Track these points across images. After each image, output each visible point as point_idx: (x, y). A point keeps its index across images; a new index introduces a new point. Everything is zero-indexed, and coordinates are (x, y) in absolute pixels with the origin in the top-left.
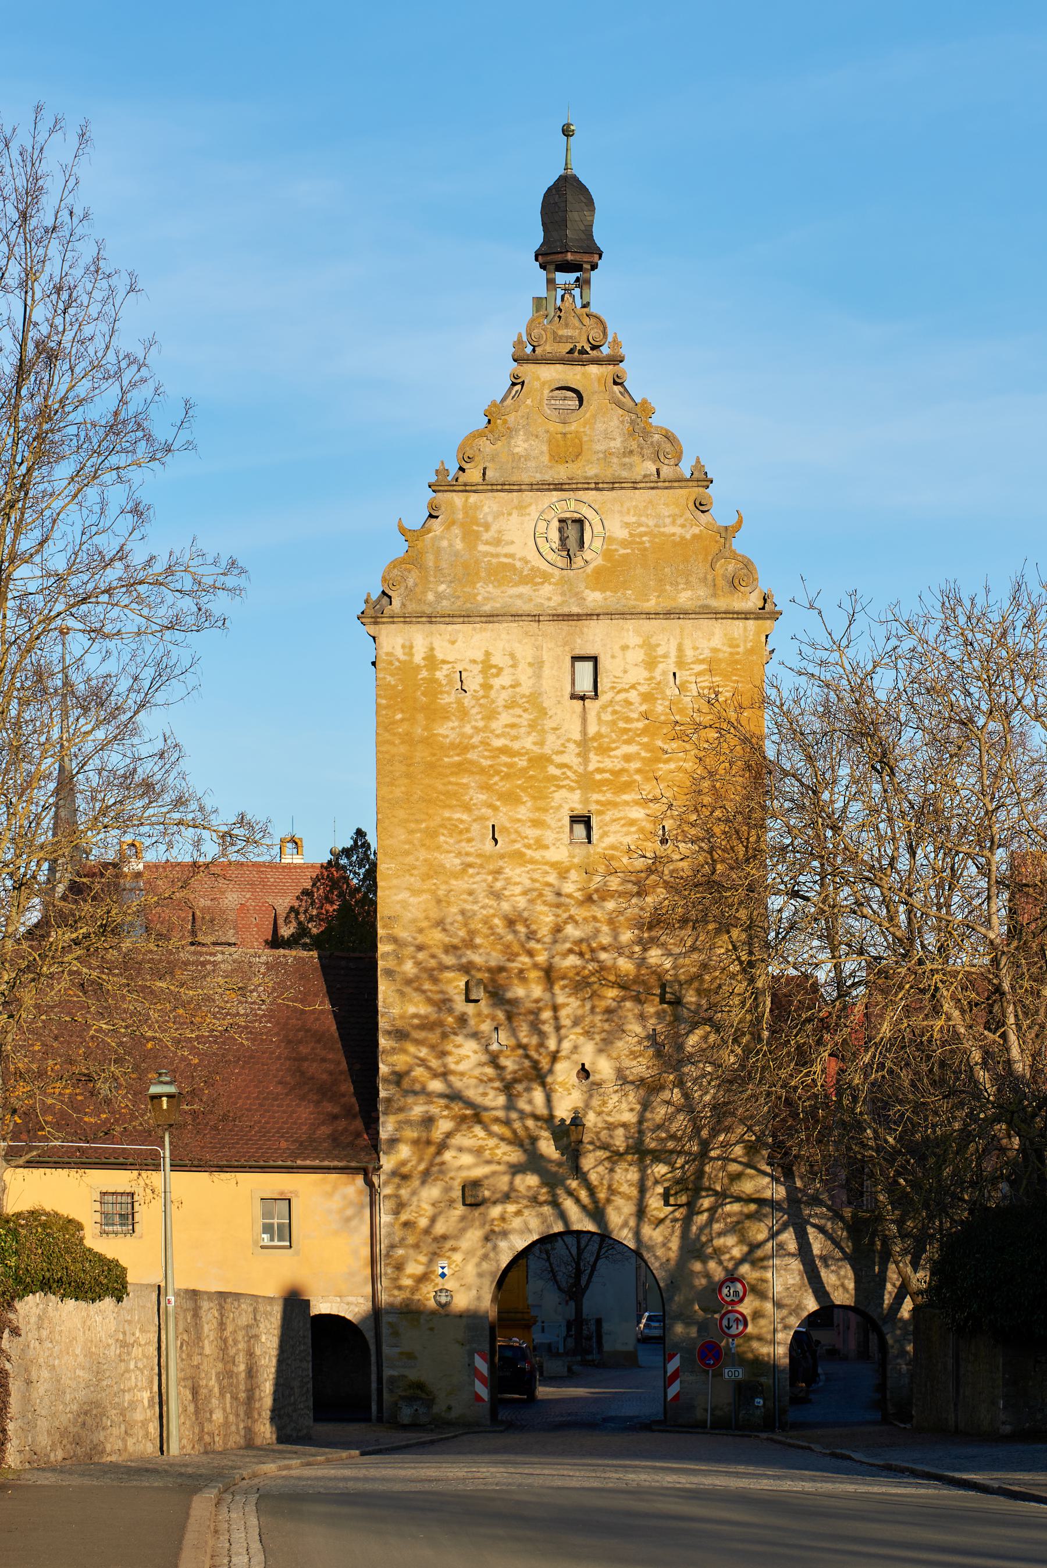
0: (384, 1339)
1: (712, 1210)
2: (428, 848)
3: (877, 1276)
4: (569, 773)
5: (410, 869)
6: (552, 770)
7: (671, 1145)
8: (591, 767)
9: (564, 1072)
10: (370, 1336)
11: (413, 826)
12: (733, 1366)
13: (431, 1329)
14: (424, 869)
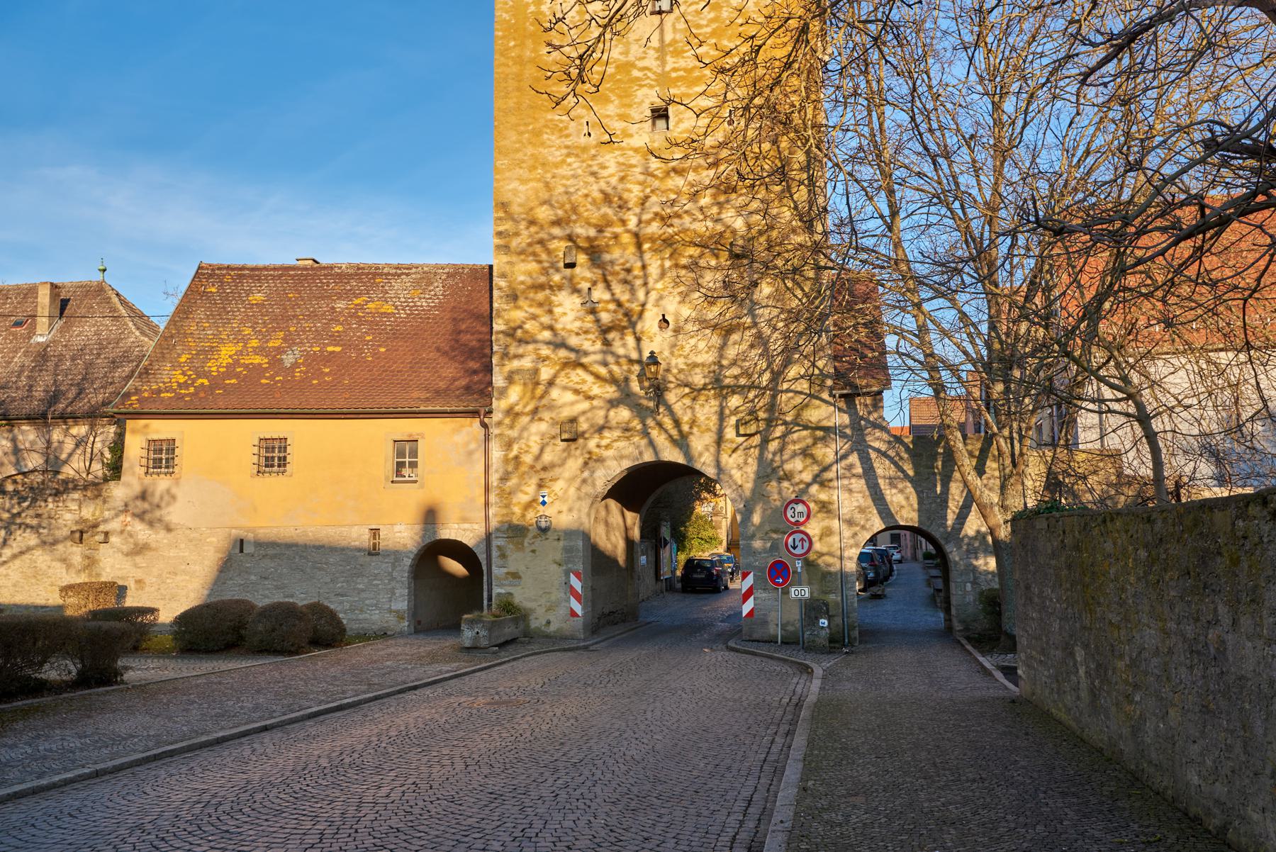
0: (494, 560)
1: (783, 436)
2: (534, 145)
3: (938, 496)
4: (649, 74)
5: (519, 164)
6: (636, 73)
7: (743, 381)
8: (668, 68)
9: (650, 323)
10: (482, 557)
11: (522, 128)
12: (800, 584)
13: (533, 551)
14: (531, 162)
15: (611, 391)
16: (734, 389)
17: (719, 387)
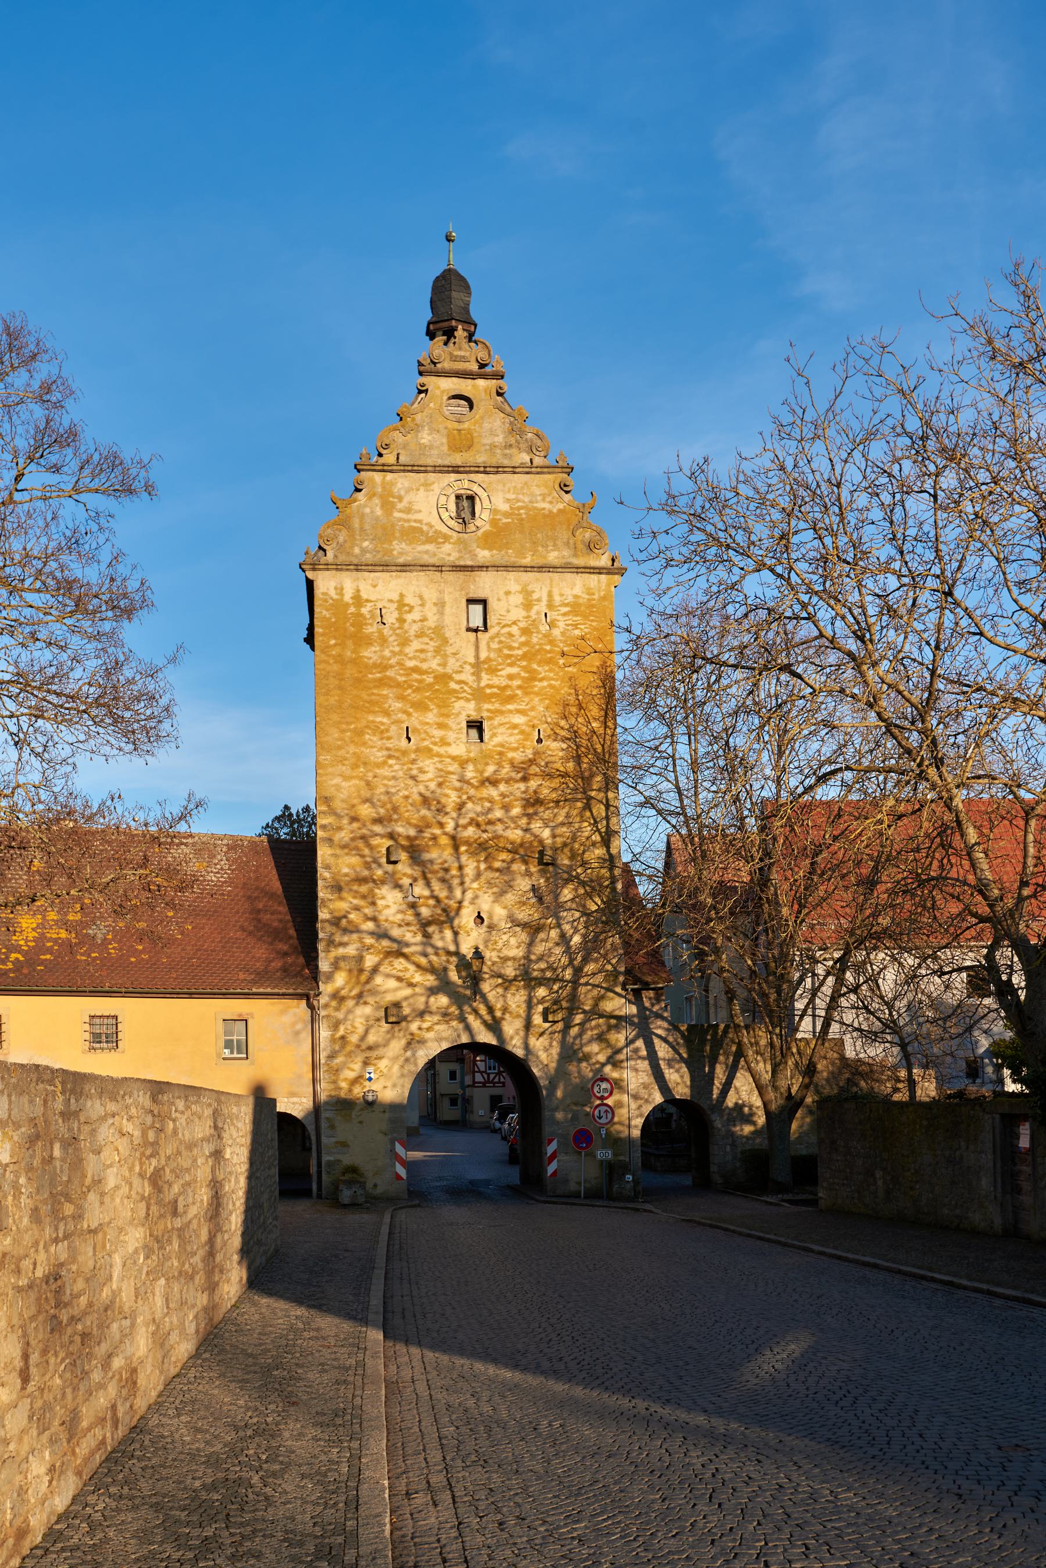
1: (582, 1024)
2: (356, 744)
5: (342, 761)
6: (453, 685)
7: (548, 974)
8: (483, 684)
9: (466, 918)
10: (311, 1128)
11: (344, 726)
14: (353, 760)
15: (430, 980)
16: (541, 982)
17: (528, 979)
